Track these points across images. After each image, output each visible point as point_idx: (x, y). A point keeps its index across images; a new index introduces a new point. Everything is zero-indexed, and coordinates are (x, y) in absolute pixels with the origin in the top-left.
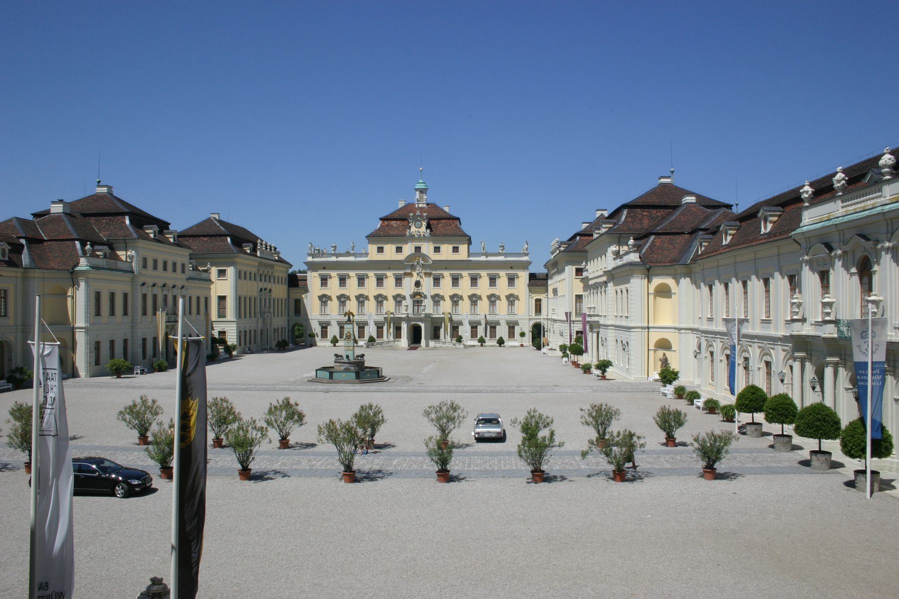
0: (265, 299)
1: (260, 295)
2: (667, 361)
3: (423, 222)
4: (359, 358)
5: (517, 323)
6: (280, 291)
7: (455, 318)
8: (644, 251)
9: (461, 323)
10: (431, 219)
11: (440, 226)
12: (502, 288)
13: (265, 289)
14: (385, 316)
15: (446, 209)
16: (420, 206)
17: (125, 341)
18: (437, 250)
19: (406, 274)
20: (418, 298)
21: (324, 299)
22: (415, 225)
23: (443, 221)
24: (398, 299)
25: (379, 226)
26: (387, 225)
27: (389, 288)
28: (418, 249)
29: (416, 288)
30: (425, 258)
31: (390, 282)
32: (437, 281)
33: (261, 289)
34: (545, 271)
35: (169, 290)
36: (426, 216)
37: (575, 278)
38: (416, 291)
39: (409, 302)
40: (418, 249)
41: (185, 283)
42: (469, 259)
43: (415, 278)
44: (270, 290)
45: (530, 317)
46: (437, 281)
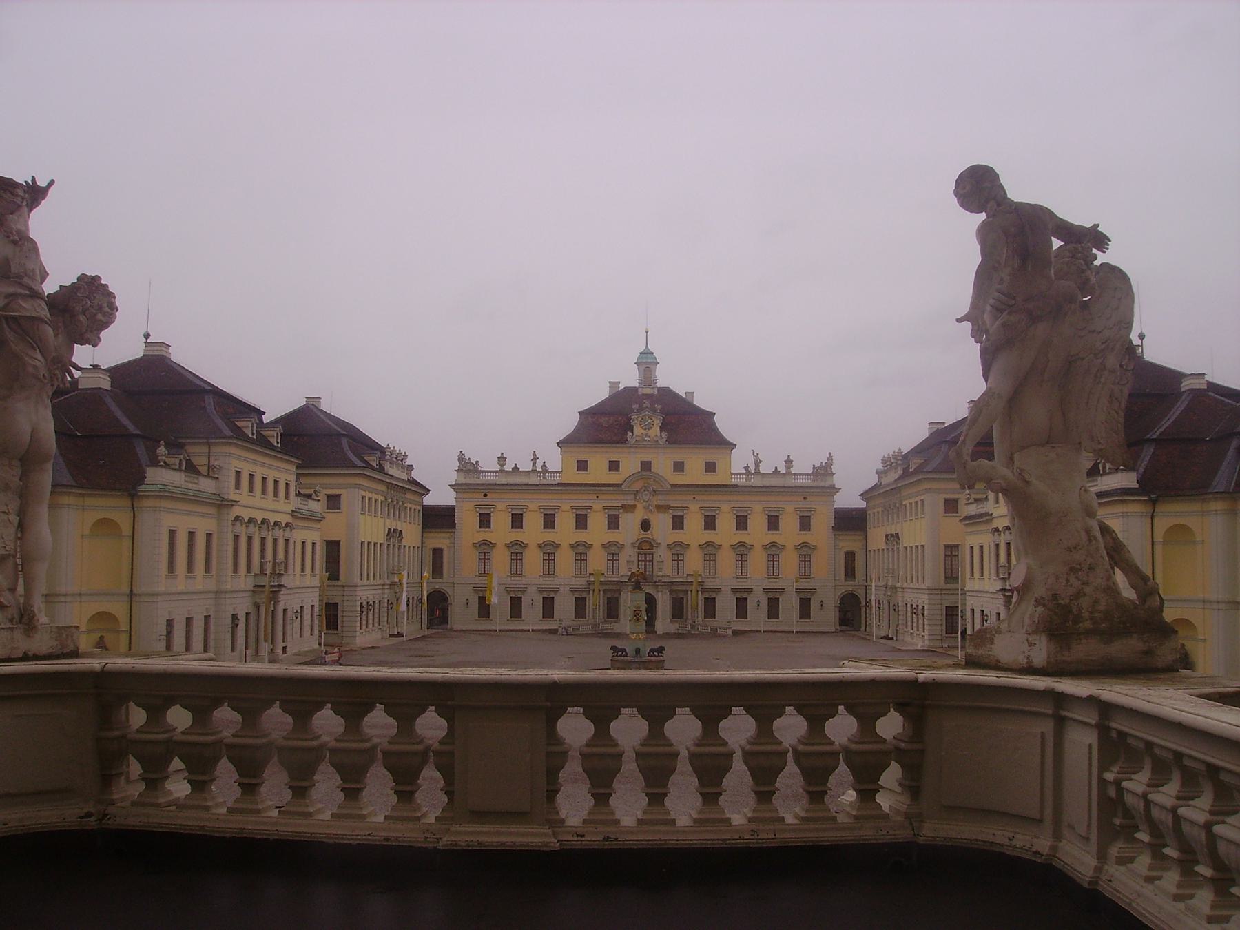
0: (394, 546)
1: (388, 540)
2: (1188, 658)
3: (654, 419)
4: (656, 654)
5: (813, 591)
6: (412, 533)
7: (709, 583)
8: (1141, 470)
9: (718, 591)
12: (789, 532)
13: (394, 530)
14: (587, 579)
16: (648, 391)
17: (207, 618)
18: (679, 467)
19: (626, 508)
20: (646, 547)
21: (485, 549)
24: (613, 550)
27: (597, 531)
28: (646, 466)
29: (643, 532)
31: (597, 521)
32: (678, 523)
33: (389, 530)
34: (862, 504)
35: (269, 531)
37: (944, 516)
38: (641, 537)
39: (628, 554)
40: (646, 466)
41: (288, 519)
43: (639, 515)
44: (401, 531)
45: (837, 583)
46: (678, 523)
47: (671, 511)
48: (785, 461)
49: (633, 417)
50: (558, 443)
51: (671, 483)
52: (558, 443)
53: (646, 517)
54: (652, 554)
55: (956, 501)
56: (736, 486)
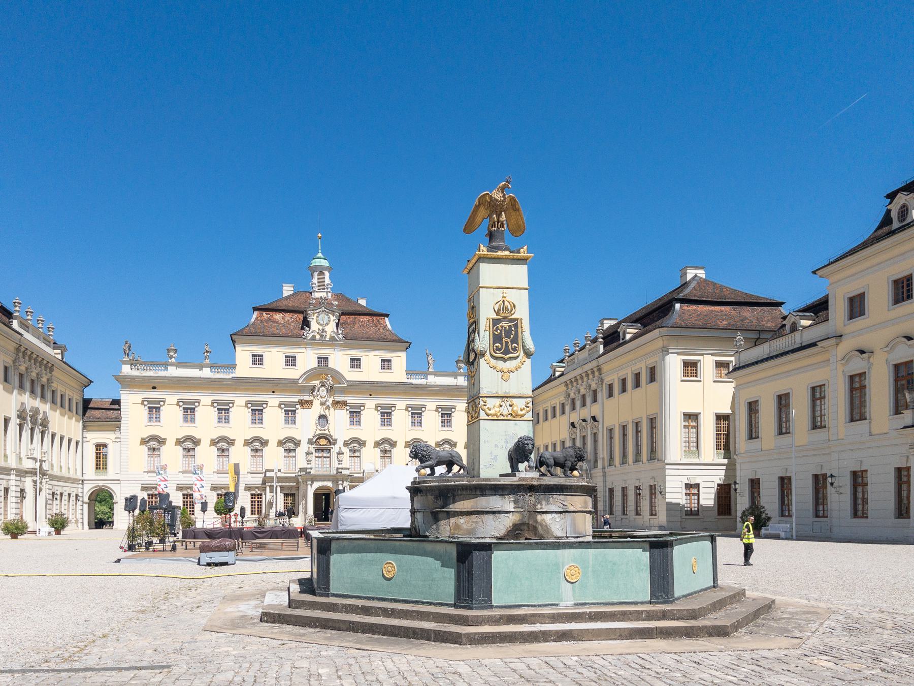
10: (343, 314)
11: (359, 325)
15: (363, 302)
18: (355, 363)
22: (317, 317)
23: (362, 318)
25: (253, 320)
26: (268, 320)
28: (323, 360)
29: (319, 428)
30: (337, 375)
31: (273, 415)
36: (337, 305)
38: (318, 432)
40: (323, 360)
42: (409, 381)
47: (348, 408)
48: (456, 361)
49: (309, 312)
50: (231, 335)
51: (347, 380)
52: (231, 335)
53: (324, 413)
54: (330, 450)
55: (694, 364)
56: (411, 384)
